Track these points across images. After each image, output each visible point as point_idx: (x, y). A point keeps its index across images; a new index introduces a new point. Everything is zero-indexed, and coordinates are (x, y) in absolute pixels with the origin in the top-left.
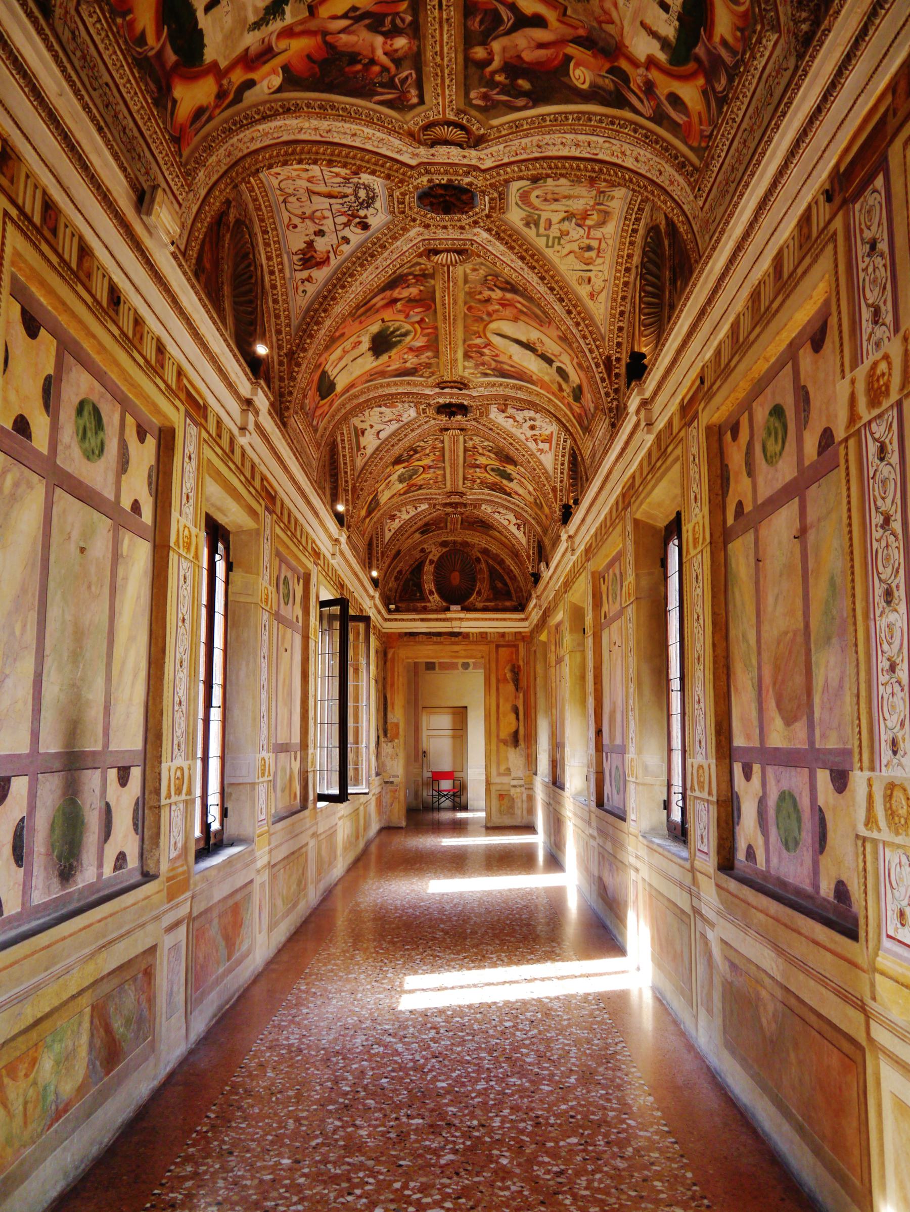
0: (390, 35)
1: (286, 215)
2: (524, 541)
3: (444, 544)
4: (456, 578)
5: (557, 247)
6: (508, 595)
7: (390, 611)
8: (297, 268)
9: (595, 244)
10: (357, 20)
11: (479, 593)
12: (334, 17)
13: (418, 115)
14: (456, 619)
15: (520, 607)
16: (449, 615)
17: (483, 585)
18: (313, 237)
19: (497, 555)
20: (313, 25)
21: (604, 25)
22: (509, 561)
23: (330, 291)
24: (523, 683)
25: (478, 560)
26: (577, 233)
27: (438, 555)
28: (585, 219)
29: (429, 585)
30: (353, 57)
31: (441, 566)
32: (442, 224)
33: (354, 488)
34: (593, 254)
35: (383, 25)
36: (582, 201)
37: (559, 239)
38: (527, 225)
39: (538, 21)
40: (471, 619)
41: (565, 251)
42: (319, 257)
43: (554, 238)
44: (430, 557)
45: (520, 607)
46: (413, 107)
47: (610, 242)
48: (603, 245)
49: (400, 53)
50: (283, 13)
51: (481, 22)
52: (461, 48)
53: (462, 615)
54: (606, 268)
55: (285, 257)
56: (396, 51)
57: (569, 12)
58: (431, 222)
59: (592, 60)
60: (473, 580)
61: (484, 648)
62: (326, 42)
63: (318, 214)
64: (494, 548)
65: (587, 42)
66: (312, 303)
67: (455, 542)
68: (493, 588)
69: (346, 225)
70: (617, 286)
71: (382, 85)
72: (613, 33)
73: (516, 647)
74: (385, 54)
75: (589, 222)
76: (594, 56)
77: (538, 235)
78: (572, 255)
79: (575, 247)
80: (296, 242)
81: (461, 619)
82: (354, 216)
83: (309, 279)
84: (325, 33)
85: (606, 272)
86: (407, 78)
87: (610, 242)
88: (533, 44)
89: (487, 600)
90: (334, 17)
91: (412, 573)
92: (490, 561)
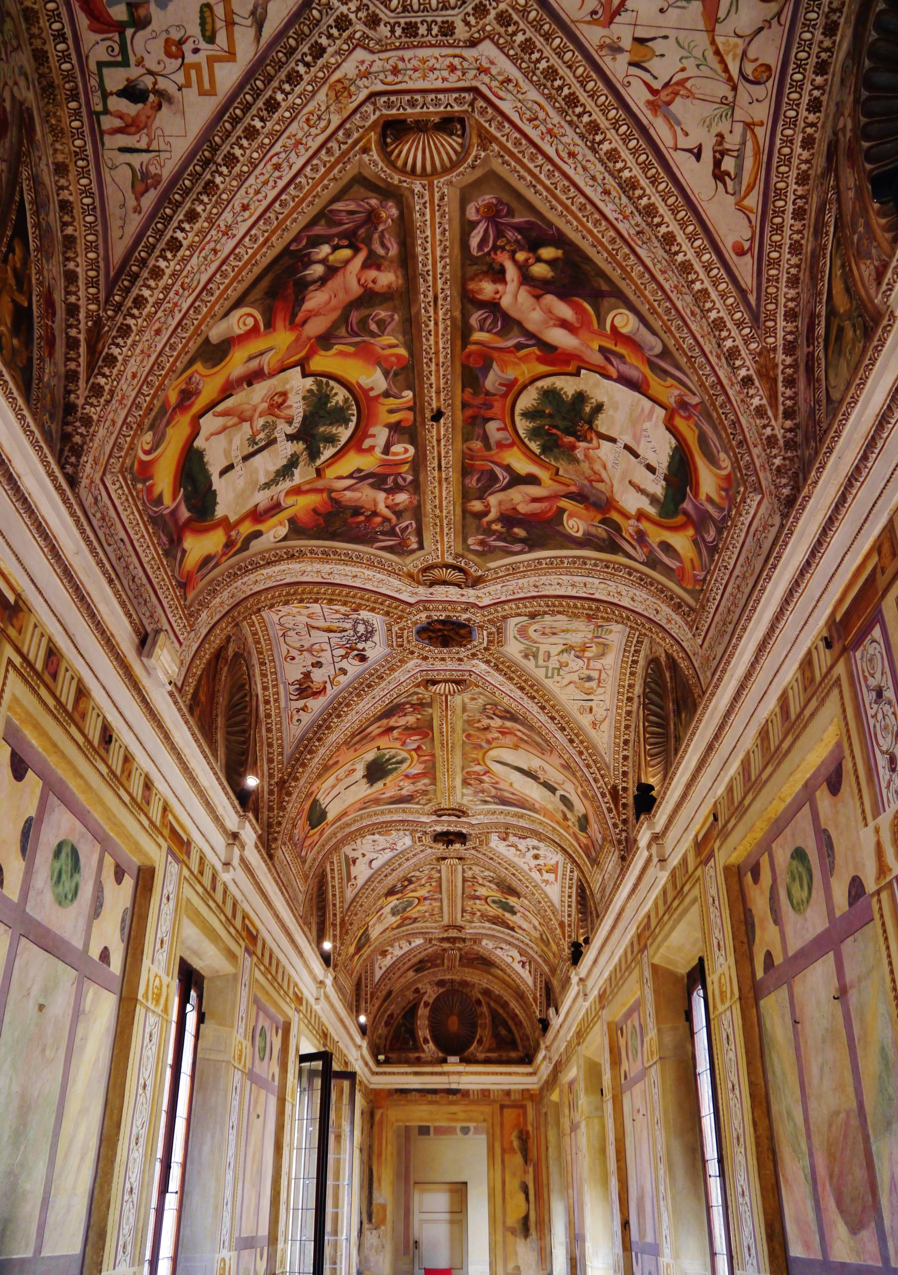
0: (391, 491)
1: (284, 648)
2: (530, 981)
3: (441, 983)
4: (453, 1024)
5: (557, 678)
6: (513, 1045)
7: (378, 1063)
8: (293, 697)
9: (595, 674)
10: (362, 479)
11: (480, 1042)
12: (341, 478)
13: (418, 559)
14: (454, 1073)
15: (527, 1059)
16: (446, 1068)
17: (484, 1032)
18: (310, 668)
19: (500, 997)
20: (320, 484)
21: (594, 484)
22: (513, 1004)
23: (325, 720)
24: (533, 1154)
25: (479, 1002)
26: (576, 664)
27: (434, 996)
28: (584, 651)
29: (423, 1032)
30: (357, 511)
31: (436, 1008)
32: (440, 656)
34: (594, 684)
35: (385, 483)
36: (581, 635)
37: (559, 670)
38: (526, 656)
39: (532, 480)
40: (472, 1073)
41: (565, 682)
42: (316, 687)
43: (554, 669)
44: (425, 998)
45: (527, 1059)
46: (413, 551)
47: (610, 673)
48: (604, 676)
49: (401, 507)
50: (293, 475)
51: (478, 480)
52: (459, 501)
53: (461, 1068)
54: (607, 697)
55: (281, 687)
56: (398, 504)
57: (561, 473)
58: (429, 655)
59: (584, 512)
60: (474, 1026)
61: (487, 1109)
62: (332, 499)
63: (316, 647)
64: (497, 989)
65: (580, 497)
66: (307, 732)
67: (452, 981)
68: (496, 1035)
69: (344, 657)
70: (620, 715)
71: (383, 533)
72: (603, 489)
73: (524, 1107)
74: (387, 507)
75: (587, 654)
76: (587, 508)
77: (537, 666)
78: (572, 685)
79: (575, 677)
80: (293, 672)
81: (460, 1073)
82: (352, 649)
83: (304, 709)
84: (331, 491)
85: (608, 702)
86: (407, 527)
87: (610, 673)
88: (528, 498)
89: (490, 1050)
90: (341, 478)
91: (404, 1017)
92: (492, 1004)
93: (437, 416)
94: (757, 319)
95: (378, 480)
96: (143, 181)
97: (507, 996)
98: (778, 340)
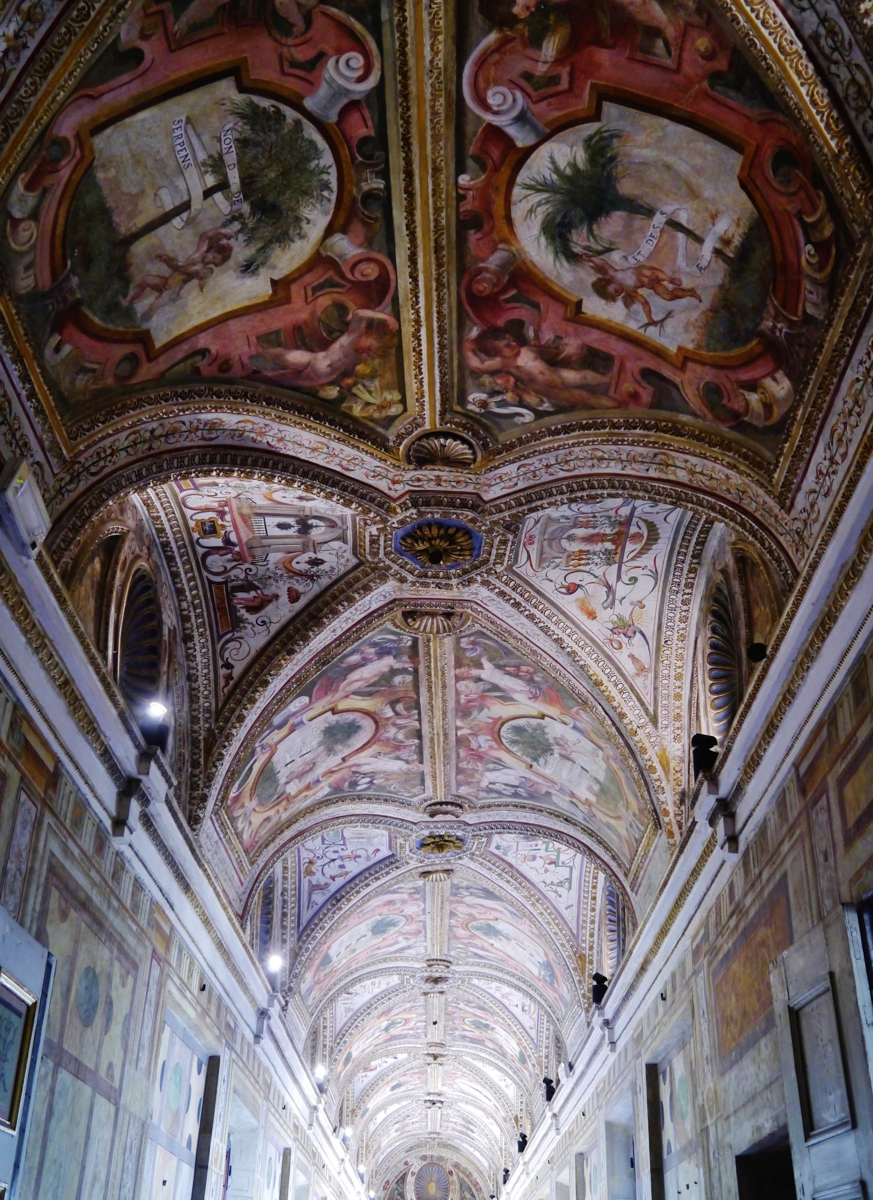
2: (486, 1164)
3: (424, 1158)
22: (475, 1175)
25: (451, 1173)
31: (419, 1177)
33: (367, 1145)
60: (447, 1190)
64: (464, 1164)
93: (435, 1023)
94: (537, 1047)
96: (348, 1010)
97: (471, 1169)
98: (543, 1054)
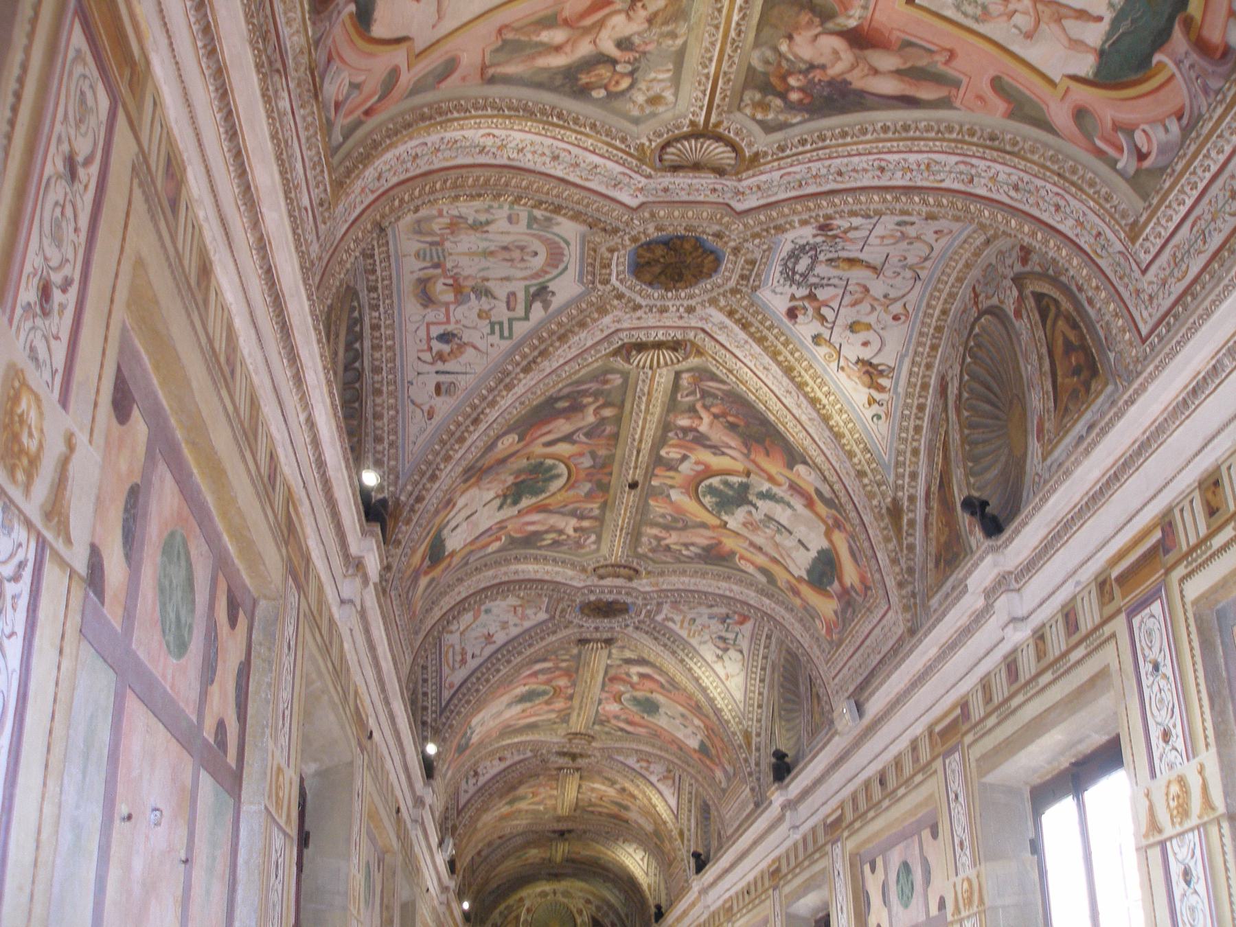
30: (732, 427)
49: (687, 415)
62: (749, 450)
71: (715, 396)
95: (701, 440)
